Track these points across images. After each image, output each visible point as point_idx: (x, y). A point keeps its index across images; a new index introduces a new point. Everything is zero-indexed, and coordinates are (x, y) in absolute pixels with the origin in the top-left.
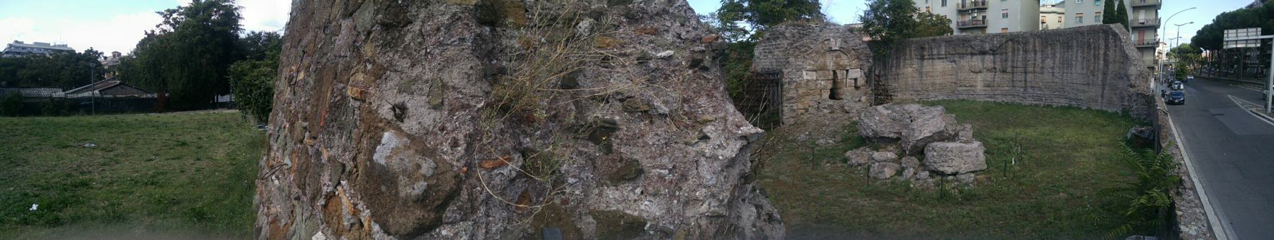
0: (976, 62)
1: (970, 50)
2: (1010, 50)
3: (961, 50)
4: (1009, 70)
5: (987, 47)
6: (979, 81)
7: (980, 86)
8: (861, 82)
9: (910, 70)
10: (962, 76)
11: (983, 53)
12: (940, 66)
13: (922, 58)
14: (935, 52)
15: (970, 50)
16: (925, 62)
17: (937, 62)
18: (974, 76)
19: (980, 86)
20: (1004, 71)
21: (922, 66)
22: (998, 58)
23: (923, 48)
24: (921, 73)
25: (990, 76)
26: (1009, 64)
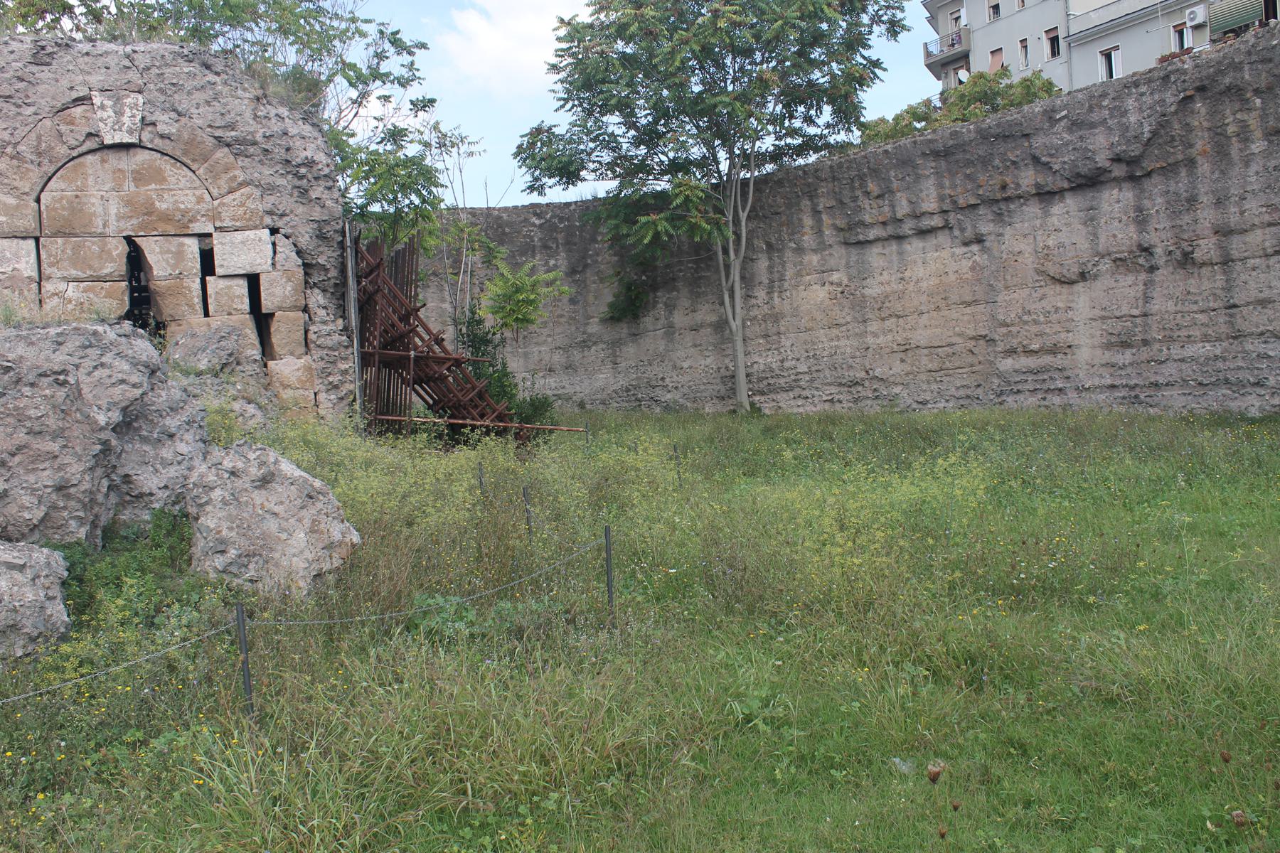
1: (1028, 178)
2: (1201, 142)
4: (1206, 248)
5: (1101, 145)
6: (1083, 319)
7: (1087, 350)
9: (820, 294)
10: (1011, 302)
11: (1089, 182)
12: (934, 263)
16: (875, 256)
17: (914, 247)
18: (1057, 297)
19: (1087, 350)
20: (1186, 261)
21: (862, 274)
22: (1156, 196)
25: (1126, 288)
26: (1207, 216)
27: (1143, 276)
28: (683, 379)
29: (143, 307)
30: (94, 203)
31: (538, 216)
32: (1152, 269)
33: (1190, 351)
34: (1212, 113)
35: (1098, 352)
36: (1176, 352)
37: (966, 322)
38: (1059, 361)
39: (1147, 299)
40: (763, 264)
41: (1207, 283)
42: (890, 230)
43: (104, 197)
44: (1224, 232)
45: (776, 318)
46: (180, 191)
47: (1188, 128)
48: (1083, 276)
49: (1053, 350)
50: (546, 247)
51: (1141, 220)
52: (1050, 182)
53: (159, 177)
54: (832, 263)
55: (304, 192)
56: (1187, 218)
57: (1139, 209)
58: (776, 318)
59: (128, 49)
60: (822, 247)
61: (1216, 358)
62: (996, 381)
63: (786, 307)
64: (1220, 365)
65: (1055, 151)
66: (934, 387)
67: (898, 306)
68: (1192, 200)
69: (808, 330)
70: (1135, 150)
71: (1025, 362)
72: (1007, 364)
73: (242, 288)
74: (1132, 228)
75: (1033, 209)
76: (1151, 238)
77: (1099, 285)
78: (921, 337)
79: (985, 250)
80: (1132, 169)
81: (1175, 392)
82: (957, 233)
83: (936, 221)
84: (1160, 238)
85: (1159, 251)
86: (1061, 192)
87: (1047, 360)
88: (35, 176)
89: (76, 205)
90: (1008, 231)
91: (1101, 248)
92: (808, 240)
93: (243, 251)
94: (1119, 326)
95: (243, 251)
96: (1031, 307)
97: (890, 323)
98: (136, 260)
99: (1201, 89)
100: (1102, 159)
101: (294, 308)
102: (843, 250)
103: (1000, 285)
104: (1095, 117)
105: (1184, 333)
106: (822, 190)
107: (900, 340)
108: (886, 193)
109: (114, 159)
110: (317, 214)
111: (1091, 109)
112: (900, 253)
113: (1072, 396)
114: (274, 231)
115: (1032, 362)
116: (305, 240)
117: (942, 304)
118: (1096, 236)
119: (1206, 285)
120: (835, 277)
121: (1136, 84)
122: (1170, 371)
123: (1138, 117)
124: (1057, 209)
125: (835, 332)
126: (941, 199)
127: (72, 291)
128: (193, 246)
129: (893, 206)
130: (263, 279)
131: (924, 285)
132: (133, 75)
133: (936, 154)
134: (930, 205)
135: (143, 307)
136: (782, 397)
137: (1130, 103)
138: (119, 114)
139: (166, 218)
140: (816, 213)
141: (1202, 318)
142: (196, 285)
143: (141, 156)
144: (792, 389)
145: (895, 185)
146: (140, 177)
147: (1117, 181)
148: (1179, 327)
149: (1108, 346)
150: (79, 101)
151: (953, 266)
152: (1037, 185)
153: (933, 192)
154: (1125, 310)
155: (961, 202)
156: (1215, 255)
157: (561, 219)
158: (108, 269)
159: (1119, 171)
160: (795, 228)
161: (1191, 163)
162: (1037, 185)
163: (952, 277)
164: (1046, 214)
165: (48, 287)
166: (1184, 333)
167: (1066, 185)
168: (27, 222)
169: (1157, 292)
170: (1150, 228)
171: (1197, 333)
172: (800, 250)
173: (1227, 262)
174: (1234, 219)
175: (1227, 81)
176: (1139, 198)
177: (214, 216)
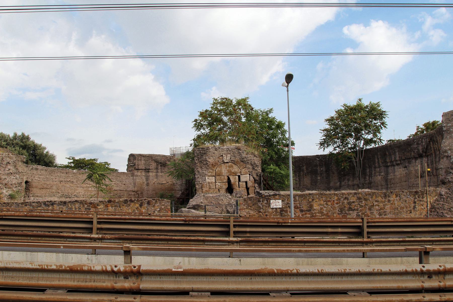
9: (379, 178)
17: (396, 167)
24: (386, 180)
29: (230, 189)
30: (224, 171)
31: (318, 158)
40: (368, 170)
43: (224, 170)
46: (235, 169)
50: (320, 165)
60: (379, 167)
73: (244, 184)
90: (410, 165)
93: (245, 178)
95: (245, 178)
96: (415, 183)
97: (392, 185)
98: (229, 179)
101: (253, 187)
114: (250, 175)
120: (382, 174)
126: (399, 157)
127: (219, 184)
128: (237, 177)
132: (229, 152)
134: (398, 158)
135: (230, 189)
138: (227, 158)
139: (233, 173)
140: (378, 159)
142: (238, 183)
143: (230, 164)
146: (229, 167)
150: (221, 156)
157: (324, 159)
158: (225, 181)
160: (374, 163)
163: (402, 175)
167: (417, 156)
172: (375, 167)
177: (241, 172)
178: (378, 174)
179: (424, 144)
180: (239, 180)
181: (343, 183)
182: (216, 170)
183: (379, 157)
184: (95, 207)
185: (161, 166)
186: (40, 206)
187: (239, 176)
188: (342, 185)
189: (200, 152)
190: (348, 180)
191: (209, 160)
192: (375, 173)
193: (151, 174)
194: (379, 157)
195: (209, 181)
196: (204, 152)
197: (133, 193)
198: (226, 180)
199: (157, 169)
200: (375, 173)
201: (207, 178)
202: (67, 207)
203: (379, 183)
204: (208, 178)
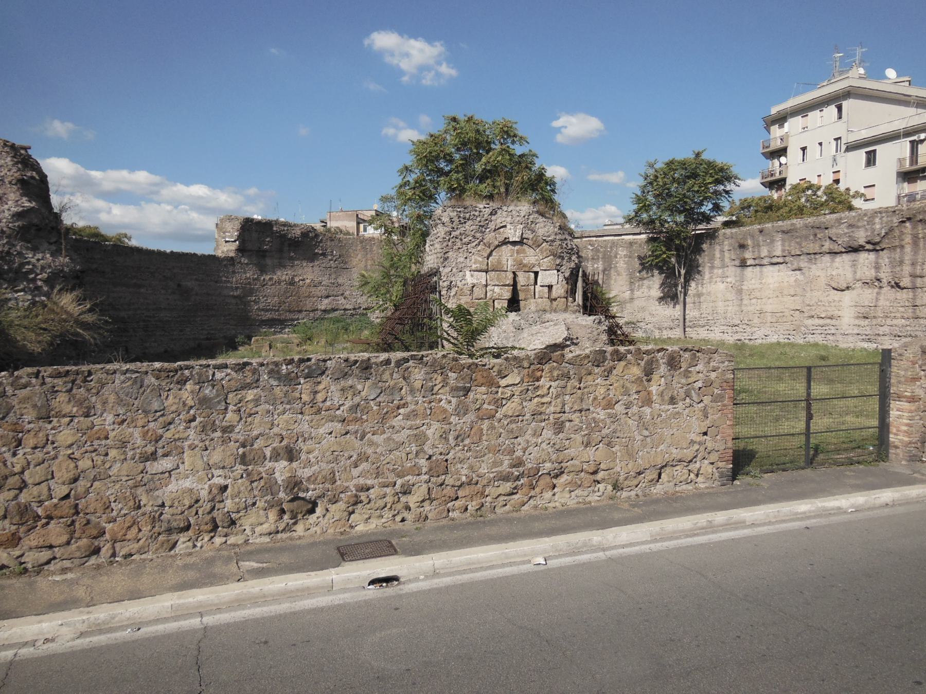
0: (842, 268)
1: (827, 245)
2: (908, 239)
3: (813, 247)
4: (906, 282)
6: (846, 307)
7: (847, 318)
8: (560, 290)
9: (721, 286)
11: (855, 250)
12: (775, 277)
13: (743, 264)
14: (764, 252)
15: (827, 245)
20: (897, 285)
22: (885, 257)
23: (742, 246)
24: (740, 292)
25: (868, 295)
27: (876, 290)
28: (654, 320)
32: (881, 287)
33: (895, 322)
34: (914, 228)
35: (852, 320)
36: (889, 322)
37: (791, 303)
38: (833, 322)
39: (877, 300)
41: (904, 295)
42: (757, 262)
44: (914, 276)
45: (699, 295)
46: (531, 256)
47: (902, 233)
48: (848, 288)
49: (831, 318)
51: (877, 268)
52: (836, 248)
53: (524, 251)
54: (728, 274)
55: (570, 258)
56: (898, 269)
57: (877, 263)
58: (699, 295)
59: (518, 209)
60: (724, 266)
61: (907, 326)
62: (803, 328)
63: (704, 291)
64: (908, 328)
65: (837, 235)
66: (773, 329)
67: (758, 294)
68: (901, 262)
69: (714, 302)
70: (877, 239)
71: (817, 321)
72: (810, 322)
73: (546, 289)
74: (873, 272)
75: (827, 258)
76: (881, 275)
77: (855, 291)
78: (768, 308)
79: (803, 274)
80: (875, 246)
81: (886, 338)
82: (789, 265)
83: (780, 260)
84: (885, 275)
85: (885, 281)
86: (841, 252)
87: (828, 321)
88: (489, 251)
89: (499, 262)
90: (814, 267)
91: (858, 277)
92: (717, 263)
94: (863, 310)
96: (822, 299)
97: (754, 301)
99: (909, 219)
100: (862, 242)
102: (734, 269)
103: (808, 289)
104: (860, 224)
105: (893, 315)
106: (726, 243)
107: (758, 308)
108: (757, 246)
109: (510, 247)
110: (573, 265)
111: (859, 220)
112: (761, 272)
113: (840, 338)
114: (558, 271)
115: (821, 322)
116: (567, 274)
117: (780, 295)
118: (855, 272)
119: (905, 296)
120: (729, 280)
121: (880, 212)
122: (886, 329)
123: (879, 226)
124: (838, 259)
125: (727, 303)
126: (783, 251)
127: (497, 289)
128: (532, 275)
129: (759, 252)
130: (554, 288)
131: (771, 286)
133: (783, 232)
134: (778, 252)
136: (700, 330)
137: (877, 220)
139: (525, 266)
140: (722, 251)
141: (902, 309)
144: (704, 326)
145: (761, 243)
147: (869, 250)
148: (891, 312)
149: (858, 317)
151: (787, 279)
152: (830, 249)
153: (780, 248)
154: (866, 304)
155: (793, 253)
156: (909, 285)
159: (869, 247)
160: (712, 258)
161: (902, 247)
162: (830, 249)
163: (786, 284)
164: (833, 261)
165: (489, 288)
166: (893, 315)
167: (844, 250)
168: (485, 267)
169: (882, 297)
170: (881, 271)
171: (899, 315)
172: (712, 267)
173: (914, 288)
174: (918, 272)
175: (921, 217)
176: (877, 258)
178: (719, 279)
179: (878, 226)
180: (536, 283)
181: (637, 294)
182: (491, 259)
183: (726, 248)
184: (491, 383)
185: (290, 245)
186: (255, 384)
187: (536, 274)
188: (635, 296)
189: (459, 217)
190: (649, 288)
191: (478, 235)
192: (711, 278)
193: (269, 262)
194: (726, 248)
195: (475, 281)
196: (467, 216)
197: (233, 301)
198: (509, 281)
199: (281, 251)
200: (711, 278)
201: (468, 273)
202: (375, 385)
203: (720, 295)
204: (472, 276)
